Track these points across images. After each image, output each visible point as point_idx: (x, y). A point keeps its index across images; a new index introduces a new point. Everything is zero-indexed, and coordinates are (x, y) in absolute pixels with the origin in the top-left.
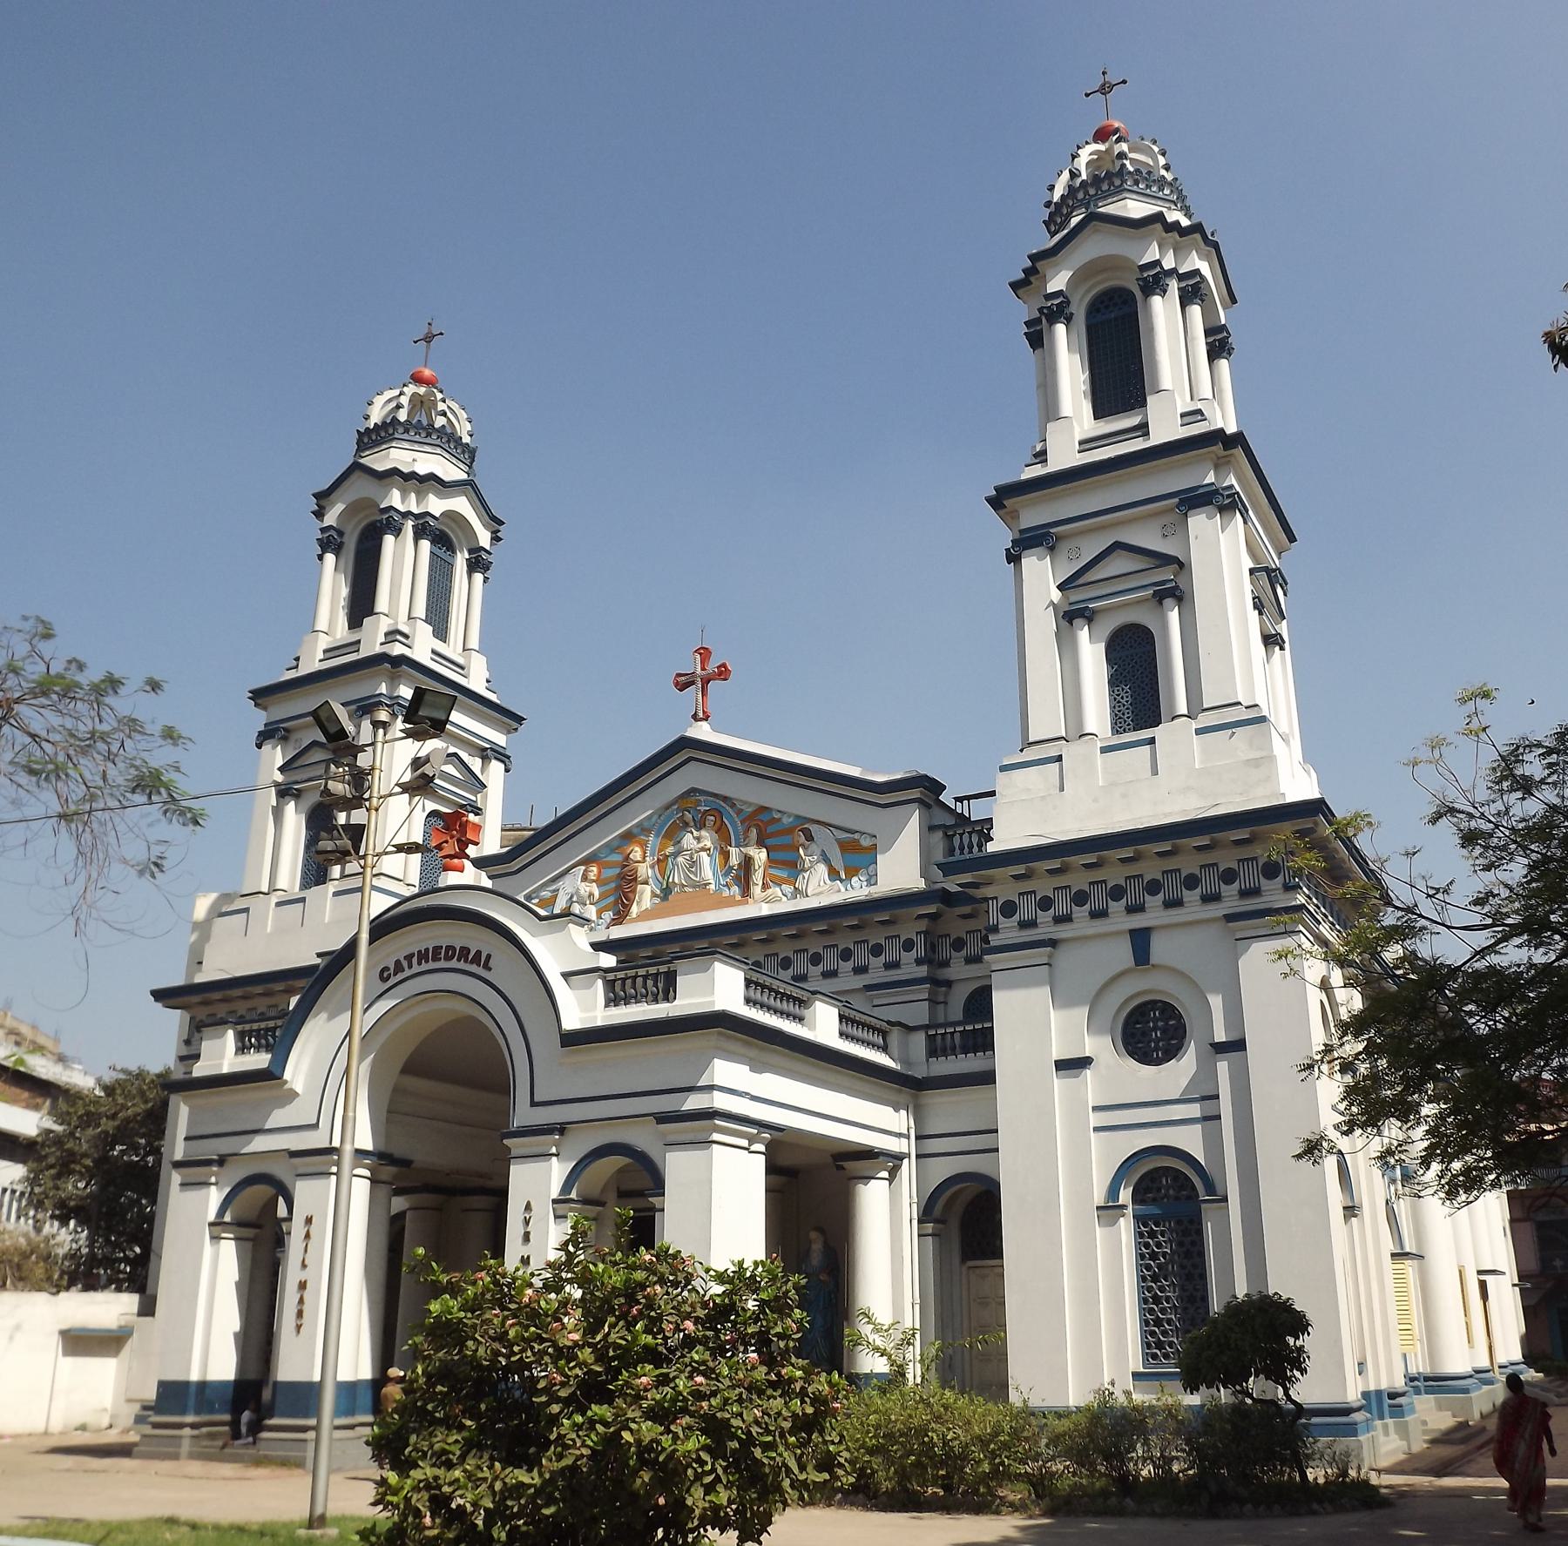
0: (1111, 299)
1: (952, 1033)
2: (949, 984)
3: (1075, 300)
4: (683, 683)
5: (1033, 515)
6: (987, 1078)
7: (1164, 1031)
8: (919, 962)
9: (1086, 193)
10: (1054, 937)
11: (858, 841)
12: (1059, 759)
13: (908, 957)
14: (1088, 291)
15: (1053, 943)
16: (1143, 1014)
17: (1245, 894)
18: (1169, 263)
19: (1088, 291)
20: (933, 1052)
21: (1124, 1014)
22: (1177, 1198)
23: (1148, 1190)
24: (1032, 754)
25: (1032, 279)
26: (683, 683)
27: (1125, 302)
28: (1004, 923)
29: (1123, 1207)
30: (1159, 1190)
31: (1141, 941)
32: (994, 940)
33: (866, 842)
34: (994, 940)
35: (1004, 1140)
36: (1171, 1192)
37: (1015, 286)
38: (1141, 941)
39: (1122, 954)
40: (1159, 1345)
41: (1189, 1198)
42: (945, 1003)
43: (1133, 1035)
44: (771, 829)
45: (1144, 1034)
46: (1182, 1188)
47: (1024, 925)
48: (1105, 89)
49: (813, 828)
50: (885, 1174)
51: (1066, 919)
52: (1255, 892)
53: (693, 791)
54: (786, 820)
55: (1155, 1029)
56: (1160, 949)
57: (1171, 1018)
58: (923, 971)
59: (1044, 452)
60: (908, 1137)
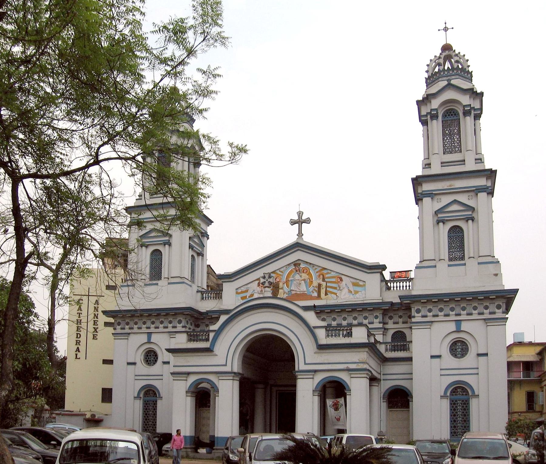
0: (450, 113)
3: (439, 112)
5: (427, 187)
6: (410, 359)
7: (462, 349)
9: (444, 73)
12: (435, 266)
14: (443, 110)
16: (456, 344)
19: (443, 110)
21: (451, 343)
22: (463, 395)
24: (425, 264)
25: (425, 101)
27: (455, 115)
28: (416, 315)
29: (448, 396)
31: (458, 323)
32: (413, 320)
35: (414, 376)
36: (461, 393)
37: (418, 102)
38: (458, 323)
39: (452, 327)
40: (455, 433)
41: (466, 395)
44: (327, 276)
45: (456, 349)
47: (423, 316)
53: (299, 260)
55: (459, 348)
59: (430, 164)
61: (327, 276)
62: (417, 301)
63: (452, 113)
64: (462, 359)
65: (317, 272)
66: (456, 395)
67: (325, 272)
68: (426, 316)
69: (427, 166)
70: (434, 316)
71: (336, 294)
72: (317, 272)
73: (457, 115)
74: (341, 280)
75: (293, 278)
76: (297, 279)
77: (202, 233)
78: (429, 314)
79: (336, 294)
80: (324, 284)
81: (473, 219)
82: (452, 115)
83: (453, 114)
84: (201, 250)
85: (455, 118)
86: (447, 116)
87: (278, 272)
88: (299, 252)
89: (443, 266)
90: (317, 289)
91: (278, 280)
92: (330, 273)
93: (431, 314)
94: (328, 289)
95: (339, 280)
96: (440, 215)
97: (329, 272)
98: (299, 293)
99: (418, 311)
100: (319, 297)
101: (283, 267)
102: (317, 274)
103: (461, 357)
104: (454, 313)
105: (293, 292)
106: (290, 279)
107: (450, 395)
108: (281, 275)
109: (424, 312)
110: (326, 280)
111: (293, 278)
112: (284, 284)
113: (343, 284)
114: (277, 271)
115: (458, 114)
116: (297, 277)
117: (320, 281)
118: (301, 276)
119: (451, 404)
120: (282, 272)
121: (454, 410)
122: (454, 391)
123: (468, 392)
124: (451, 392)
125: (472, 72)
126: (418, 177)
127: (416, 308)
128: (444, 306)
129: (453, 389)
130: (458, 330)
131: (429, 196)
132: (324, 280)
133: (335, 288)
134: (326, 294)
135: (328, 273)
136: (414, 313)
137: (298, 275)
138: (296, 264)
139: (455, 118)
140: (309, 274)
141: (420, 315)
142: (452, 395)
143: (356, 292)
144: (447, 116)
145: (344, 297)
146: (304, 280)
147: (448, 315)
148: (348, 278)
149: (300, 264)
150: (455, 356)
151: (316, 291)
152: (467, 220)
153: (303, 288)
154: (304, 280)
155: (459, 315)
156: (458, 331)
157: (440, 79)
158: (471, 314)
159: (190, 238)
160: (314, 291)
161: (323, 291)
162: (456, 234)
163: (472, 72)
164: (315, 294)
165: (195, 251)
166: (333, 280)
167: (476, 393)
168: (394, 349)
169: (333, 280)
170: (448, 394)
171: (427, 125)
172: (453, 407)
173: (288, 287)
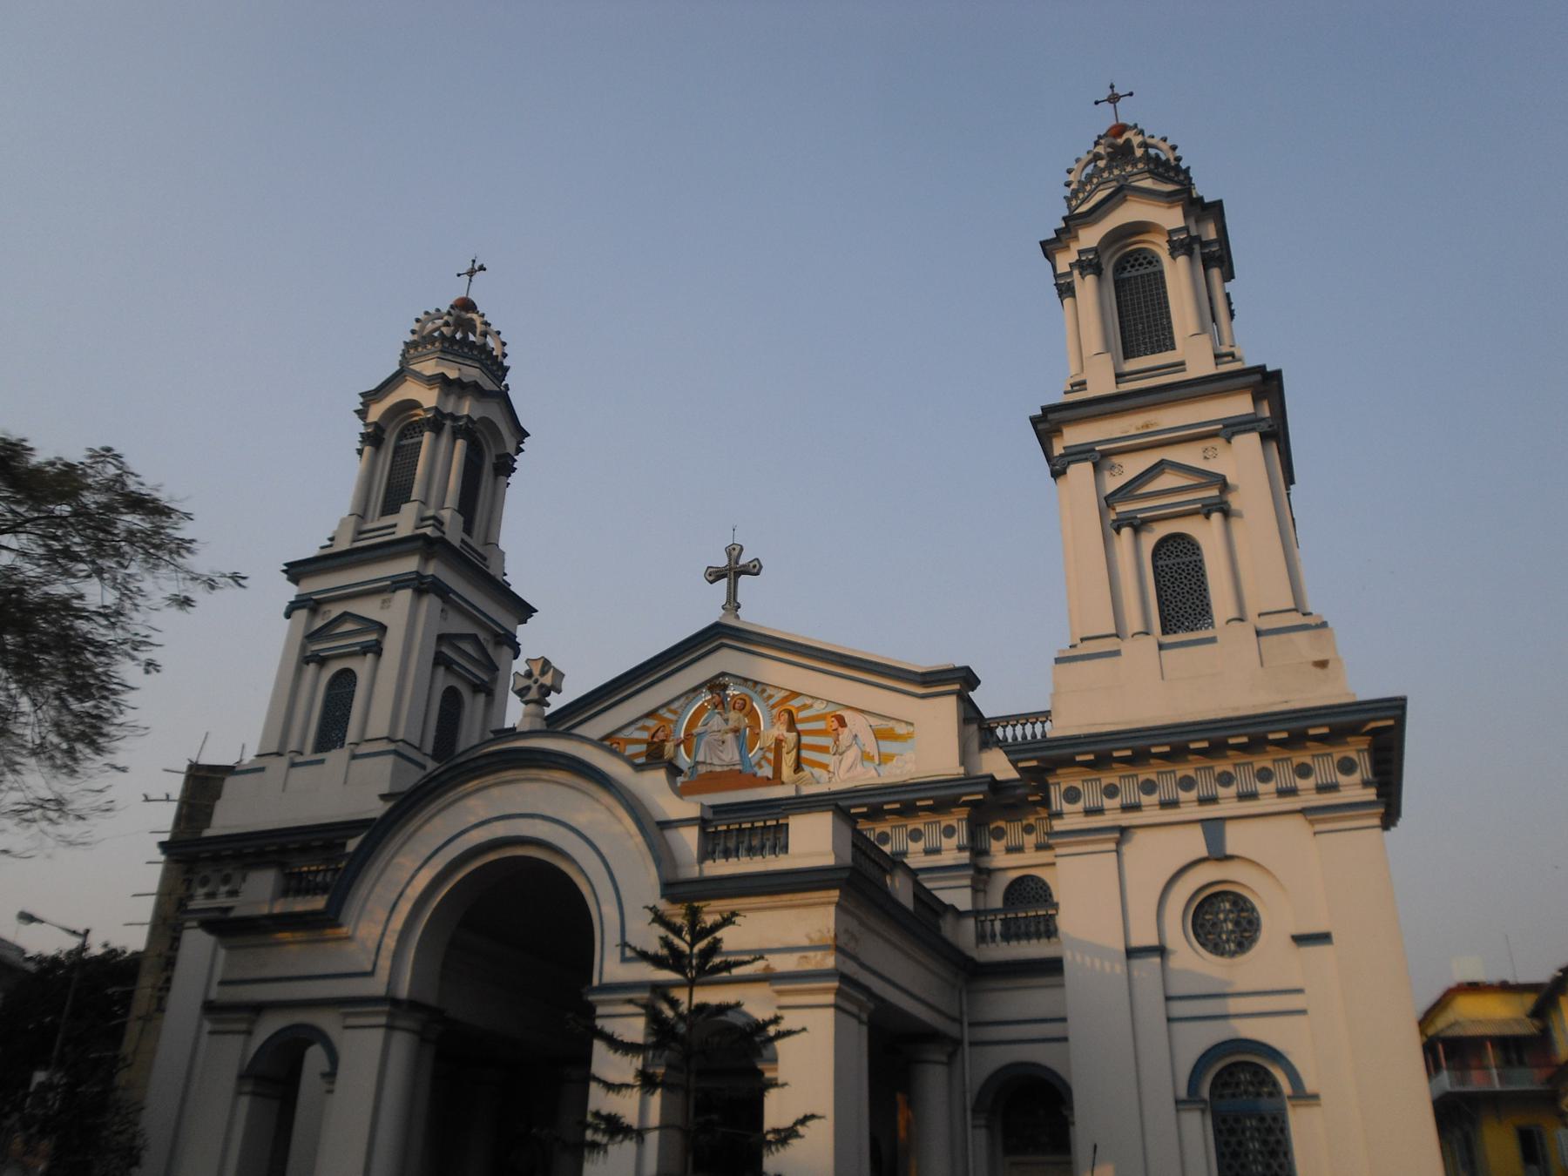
0: (1136, 260)
1: (992, 921)
2: (990, 872)
3: (1104, 261)
4: (715, 575)
7: (1237, 923)
8: (961, 849)
10: (1124, 823)
11: (892, 729)
13: (949, 843)
14: (1115, 253)
15: (1124, 832)
17: (1322, 789)
18: (1194, 233)
20: (981, 938)
23: (1226, 1085)
26: (715, 575)
27: (1150, 263)
28: (1067, 807)
30: (1238, 1085)
31: (1213, 829)
32: (1058, 825)
33: (901, 729)
34: (1058, 825)
38: (1213, 829)
39: (1194, 843)
41: (1271, 1094)
42: (985, 892)
43: (1202, 926)
44: (802, 715)
45: (1214, 924)
46: (1262, 1083)
47: (1089, 812)
48: (1114, 99)
49: (847, 715)
50: (944, 1058)
51: (1135, 807)
52: (1332, 787)
53: (723, 674)
54: (819, 708)
56: (1236, 839)
57: (1242, 910)
58: (965, 857)
60: (961, 1023)
61: (802, 715)
62: (1070, 762)
63: (1141, 260)
64: (1240, 959)
65: (773, 707)
66: (1234, 1095)
67: (796, 703)
68: (1099, 811)
69: (1075, 388)
70: (1126, 808)
71: (825, 766)
72: (773, 707)
73: (1155, 263)
74: (842, 722)
75: (704, 728)
76: (715, 728)
77: (496, 635)
78: (1108, 803)
79: (825, 766)
80: (792, 736)
81: (1227, 513)
82: (1140, 265)
83: (1145, 262)
84: (486, 678)
85: (1151, 269)
86: (1129, 269)
87: (663, 712)
88: (725, 652)
89: (1141, 652)
90: (771, 756)
91: (661, 735)
92: (811, 706)
93: (1116, 802)
94: (805, 754)
95: (835, 724)
96: (1121, 508)
97: (809, 701)
98: (718, 769)
99: (1072, 795)
100: (777, 779)
101: (678, 698)
102: (775, 711)
103: (1233, 954)
104: (1193, 794)
105: (702, 769)
106: (695, 731)
107: (1211, 1094)
108: (671, 721)
109: (1091, 797)
110: (800, 727)
111: (704, 728)
112: (678, 746)
113: (845, 735)
114: (661, 712)
115: (1159, 261)
116: (716, 722)
117: (780, 730)
118: (726, 721)
119: (1218, 1132)
120: (674, 712)
121: (1235, 1155)
122: (1225, 1081)
123: (1275, 1084)
124: (1214, 1085)
125: (1189, 168)
126: (1047, 410)
127: (1064, 786)
128: (1158, 773)
129: (1218, 1075)
130: (1218, 855)
131: (1086, 460)
132: (792, 724)
133: (823, 749)
134: (798, 768)
135: (805, 707)
136: (1057, 801)
137: (718, 716)
138: (716, 685)
139: (1151, 269)
140: (752, 714)
141: (1080, 806)
142: (1221, 1096)
143: (884, 759)
144: (1129, 269)
145: (849, 775)
146: (736, 731)
147: (1172, 804)
148: (859, 718)
149: (725, 687)
150: (1217, 949)
151: (768, 761)
152: (1206, 510)
153: (729, 755)
154: (736, 731)
155: (1211, 800)
156: (1218, 855)
157: (1101, 187)
158: (1252, 796)
159: (441, 638)
160: (763, 762)
161: (788, 761)
162: (1179, 560)
163: (1189, 168)
164: (767, 771)
165: (460, 676)
166: (820, 725)
167: (1310, 1085)
168: (1012, 933)
169: (820, 725)
170: (1205, 1092)
171: (1073, 296)
172: (1227, 1144)
173: (688, 753)
